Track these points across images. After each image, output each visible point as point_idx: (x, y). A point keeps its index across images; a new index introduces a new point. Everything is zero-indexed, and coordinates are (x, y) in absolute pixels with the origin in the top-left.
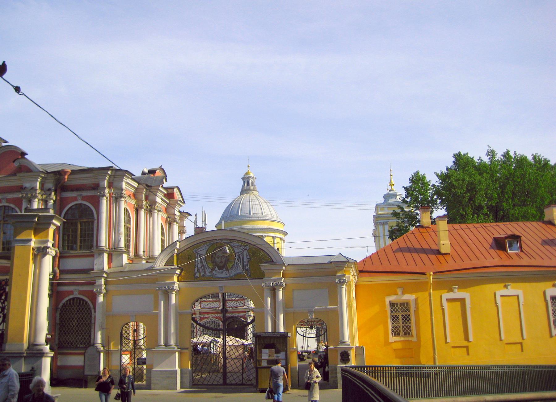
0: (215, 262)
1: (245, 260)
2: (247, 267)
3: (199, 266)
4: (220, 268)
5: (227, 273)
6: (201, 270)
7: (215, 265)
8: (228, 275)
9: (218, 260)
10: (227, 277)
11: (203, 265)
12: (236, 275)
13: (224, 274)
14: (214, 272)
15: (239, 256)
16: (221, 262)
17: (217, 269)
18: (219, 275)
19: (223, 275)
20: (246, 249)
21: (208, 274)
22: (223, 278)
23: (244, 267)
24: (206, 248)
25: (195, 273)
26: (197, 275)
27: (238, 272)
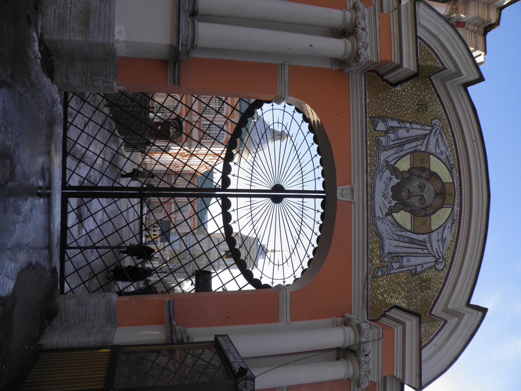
0: (409, 179)
1: (414, 261)
2: (396, 265)
3: (402, 133)
4: (396, 191)
5: (385, 211)
6: (392, 136)
7: (405, 178)
8: (378, 214)
9: (414, 185)
10: (373, 210)
11: (403, 144)
12: (378, 234)
13: (382, 202)
14: (387, 173)
15: (423, 243)
16: (410, 195)
17: (395, 181)
18: (380, 187)
19: (379, 200)
20: (436, 261)
21: (384, 155)
22: (373, 198)
23: (396, 256)
24: (442, 153)
25: (384, 121)
26: (381, 126)
27: (387, 241)
